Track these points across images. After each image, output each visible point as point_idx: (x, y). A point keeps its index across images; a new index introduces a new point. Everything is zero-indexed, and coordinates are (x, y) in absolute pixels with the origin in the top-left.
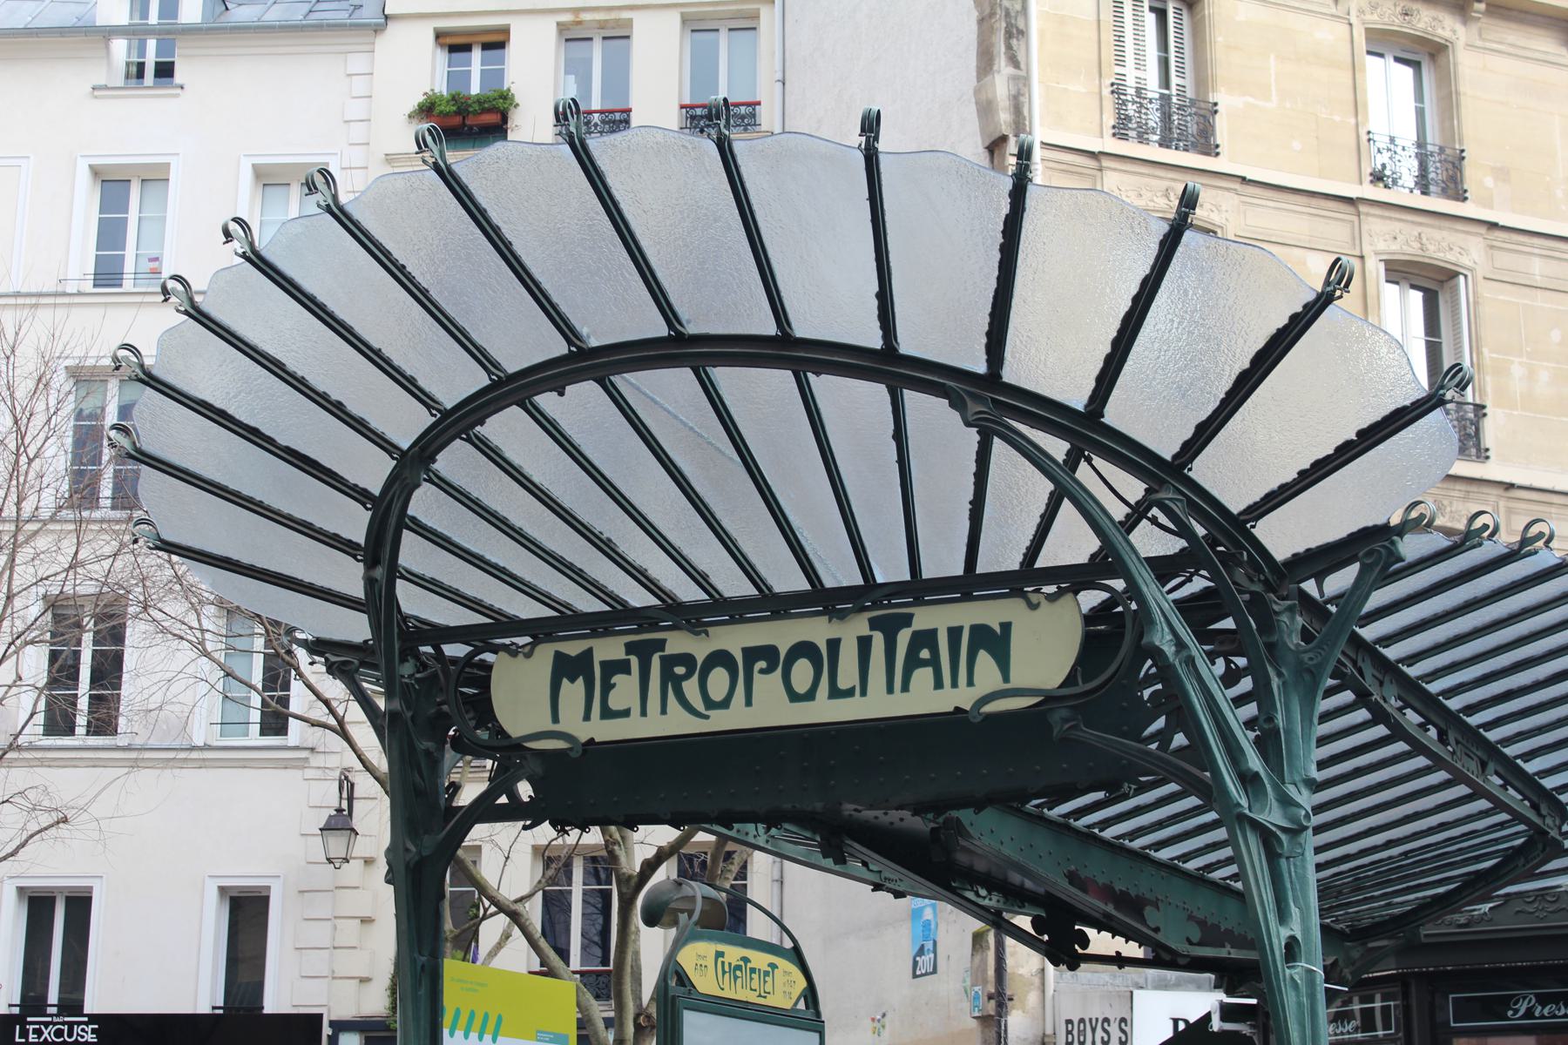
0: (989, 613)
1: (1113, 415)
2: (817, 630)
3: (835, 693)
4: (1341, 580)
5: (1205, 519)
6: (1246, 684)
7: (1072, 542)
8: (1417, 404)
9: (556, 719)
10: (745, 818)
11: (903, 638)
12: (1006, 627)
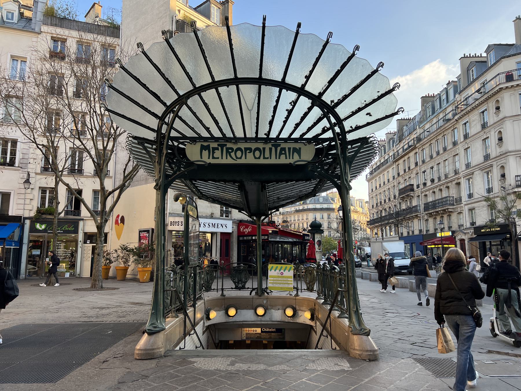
0: (297, 146)
2: (261, 146)
3: (264, 158)
9: (201, 158)
11: (279, 149)
12: (300, 148)
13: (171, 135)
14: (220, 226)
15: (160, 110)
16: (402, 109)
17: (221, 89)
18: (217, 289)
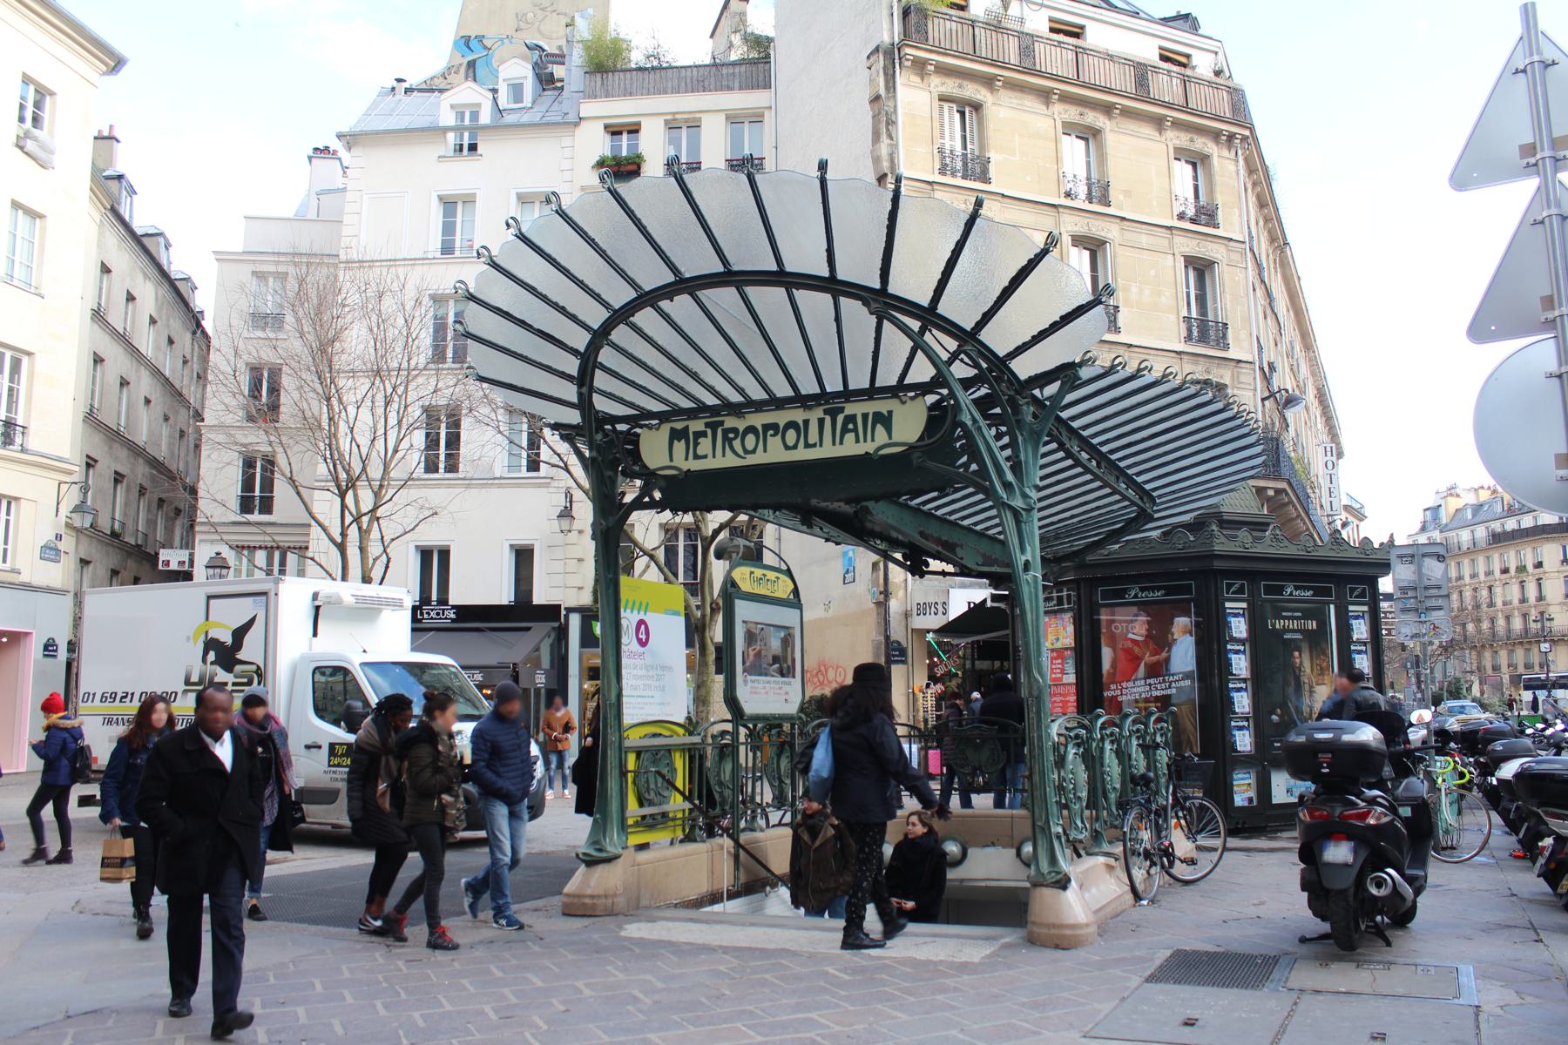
0: (882, 406)
1: (942, 309)
2: (798, 415)
3: (807, 446)
4: (1052, 389)
5: (986, 359)
6: (1006, 440)
7: (922, 371)
8: (1089, 303)
10: (764, 507)
11: (840, 418)
12: (890, 413)
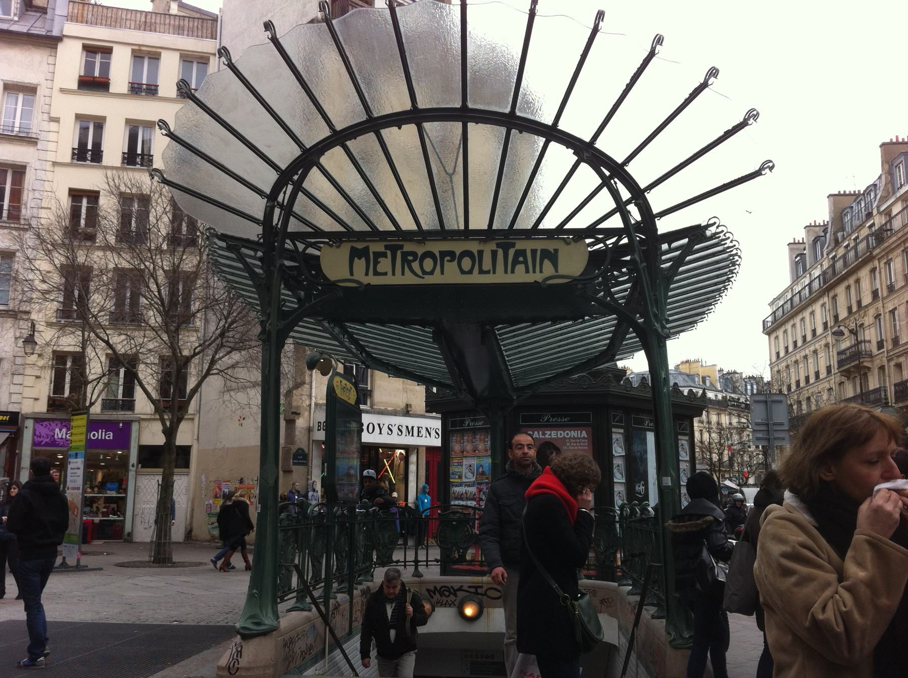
2: (473, 246)
3: (481, 272)
9: (352, 274)
11: (512, 252)
12: (556, 251)
13: (290, 229)
14: (423, 432)
15: (267, 179)
16: (771, 164)
17: (389, 134)
18: (405, 562)
